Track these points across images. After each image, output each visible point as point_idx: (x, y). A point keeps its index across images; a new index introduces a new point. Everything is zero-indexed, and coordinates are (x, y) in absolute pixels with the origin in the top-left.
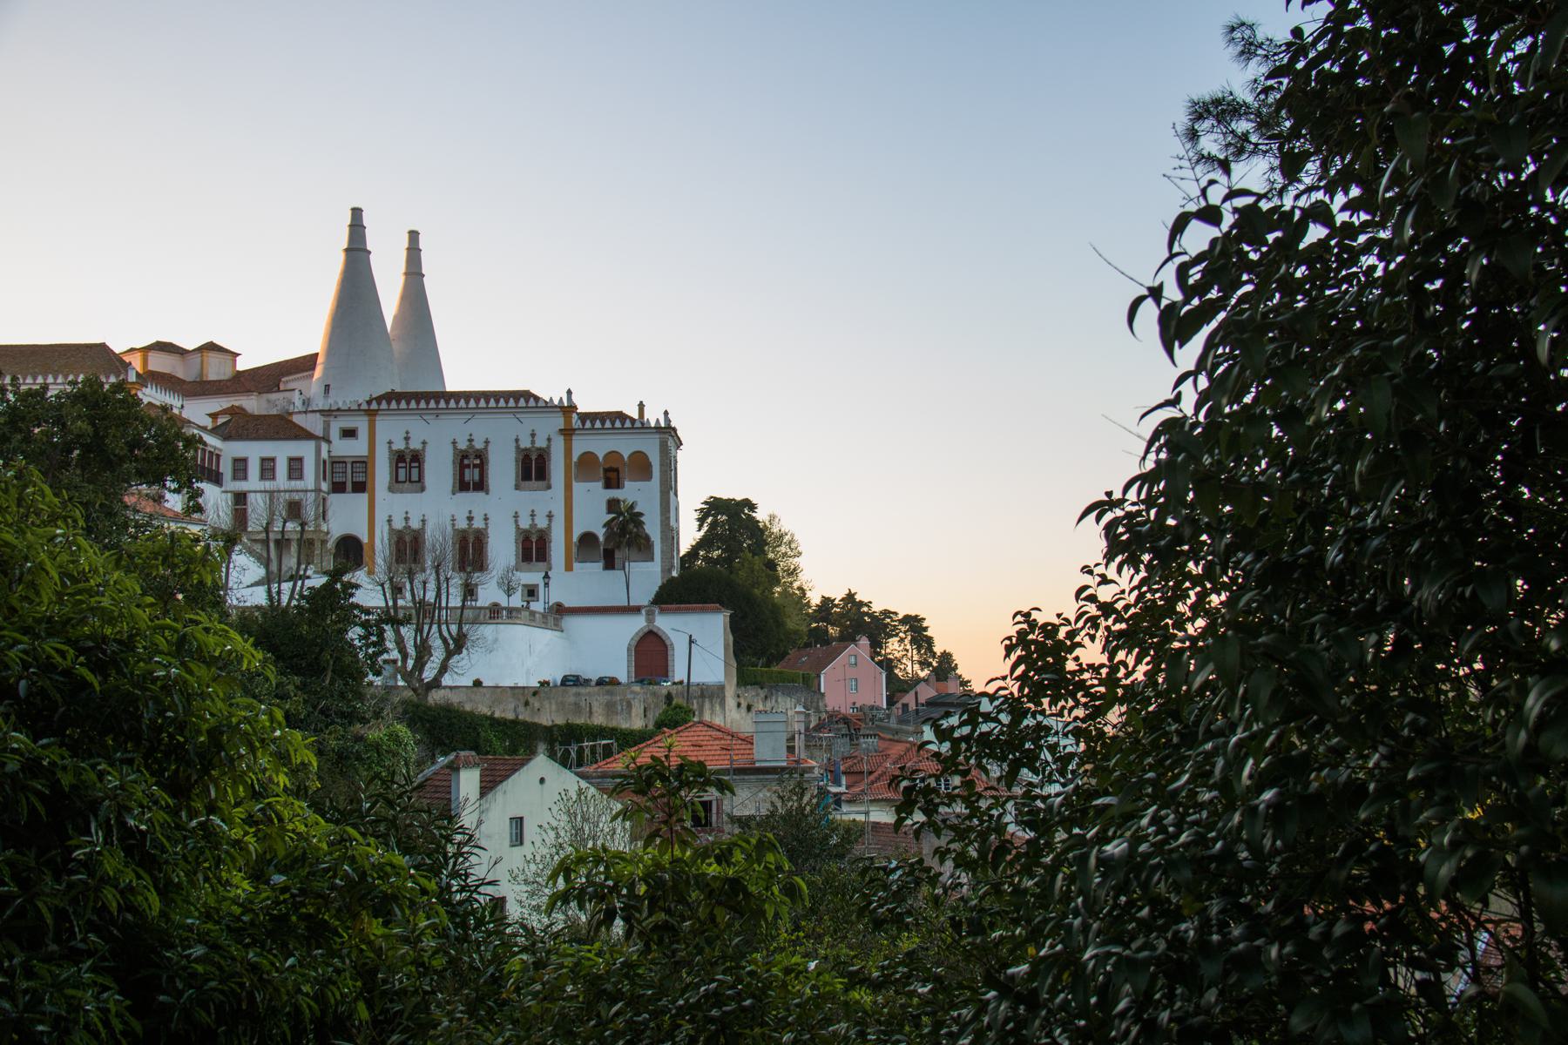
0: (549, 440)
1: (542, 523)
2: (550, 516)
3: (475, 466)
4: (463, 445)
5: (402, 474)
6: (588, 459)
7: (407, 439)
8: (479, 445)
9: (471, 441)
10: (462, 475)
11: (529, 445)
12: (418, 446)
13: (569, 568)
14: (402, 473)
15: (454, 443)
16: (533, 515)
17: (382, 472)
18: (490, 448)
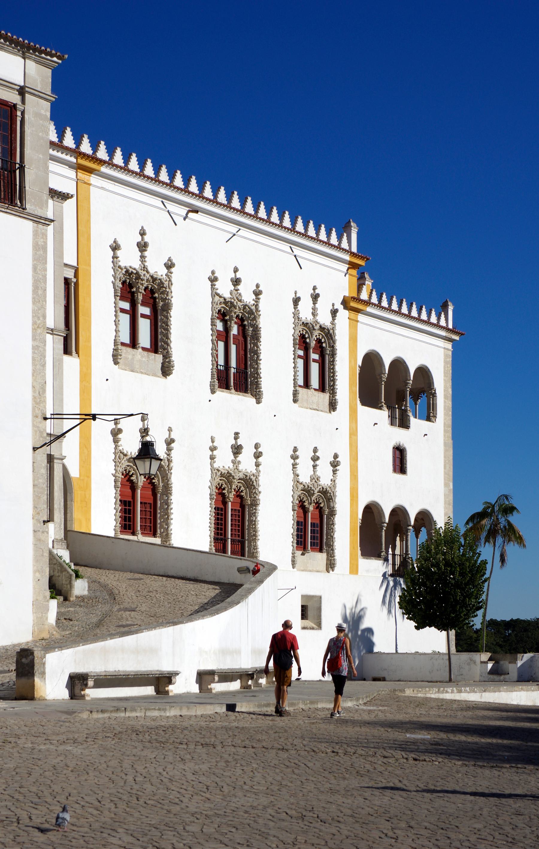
0: (334, 313)
6: (372, 360)
7: (143, 247)
9: (236, 282)
15: (213, 280)
18: (261, 307)
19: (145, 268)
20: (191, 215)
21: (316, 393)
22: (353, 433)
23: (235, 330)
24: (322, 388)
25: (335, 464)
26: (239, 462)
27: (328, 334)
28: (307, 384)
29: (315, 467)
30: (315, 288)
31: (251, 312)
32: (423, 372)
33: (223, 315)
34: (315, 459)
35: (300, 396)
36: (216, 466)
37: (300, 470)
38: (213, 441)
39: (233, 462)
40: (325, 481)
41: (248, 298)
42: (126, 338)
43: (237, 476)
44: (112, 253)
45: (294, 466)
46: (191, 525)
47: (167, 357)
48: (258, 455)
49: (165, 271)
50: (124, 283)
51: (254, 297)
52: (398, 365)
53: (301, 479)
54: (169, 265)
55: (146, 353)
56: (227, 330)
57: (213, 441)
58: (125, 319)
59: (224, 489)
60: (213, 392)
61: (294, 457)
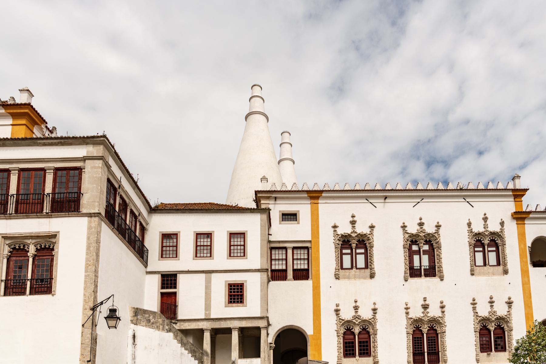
1: (501, 310)
2: (510, 303)
3: (425, 252)
4: (413, 229)
5: (347, 260)
7: (353, 223)
8: (430, 229)
9: (421, 224)
10: (411, 261)
11: (481, 230)
12: (366, 231)
14: (347, 260)
15: (404, 227)
16: (491, 302)
17: (327, 255)
18: (441, 231)
19: (354, 232)
20: (387, 200)
21: (491, 268)
26: (428, 313)
28: (485, 265)
29: (492, 306)
30: (485, 214)
31: (433, 236)
35: (475, 272)
36: (410, 316)
37: (478, 310)
38: (407, 305)
39: (423, 313)
43: (426, 319)
44: (333, 230)
45: (474, 309)
48: (442, 307)
49: (370, 230)
50: (344, 241)
51: (436, 229)
53: (480, 314)
55: (358, 270)
57: (407, 305)
59: (421, 327)
60: (406, 280)
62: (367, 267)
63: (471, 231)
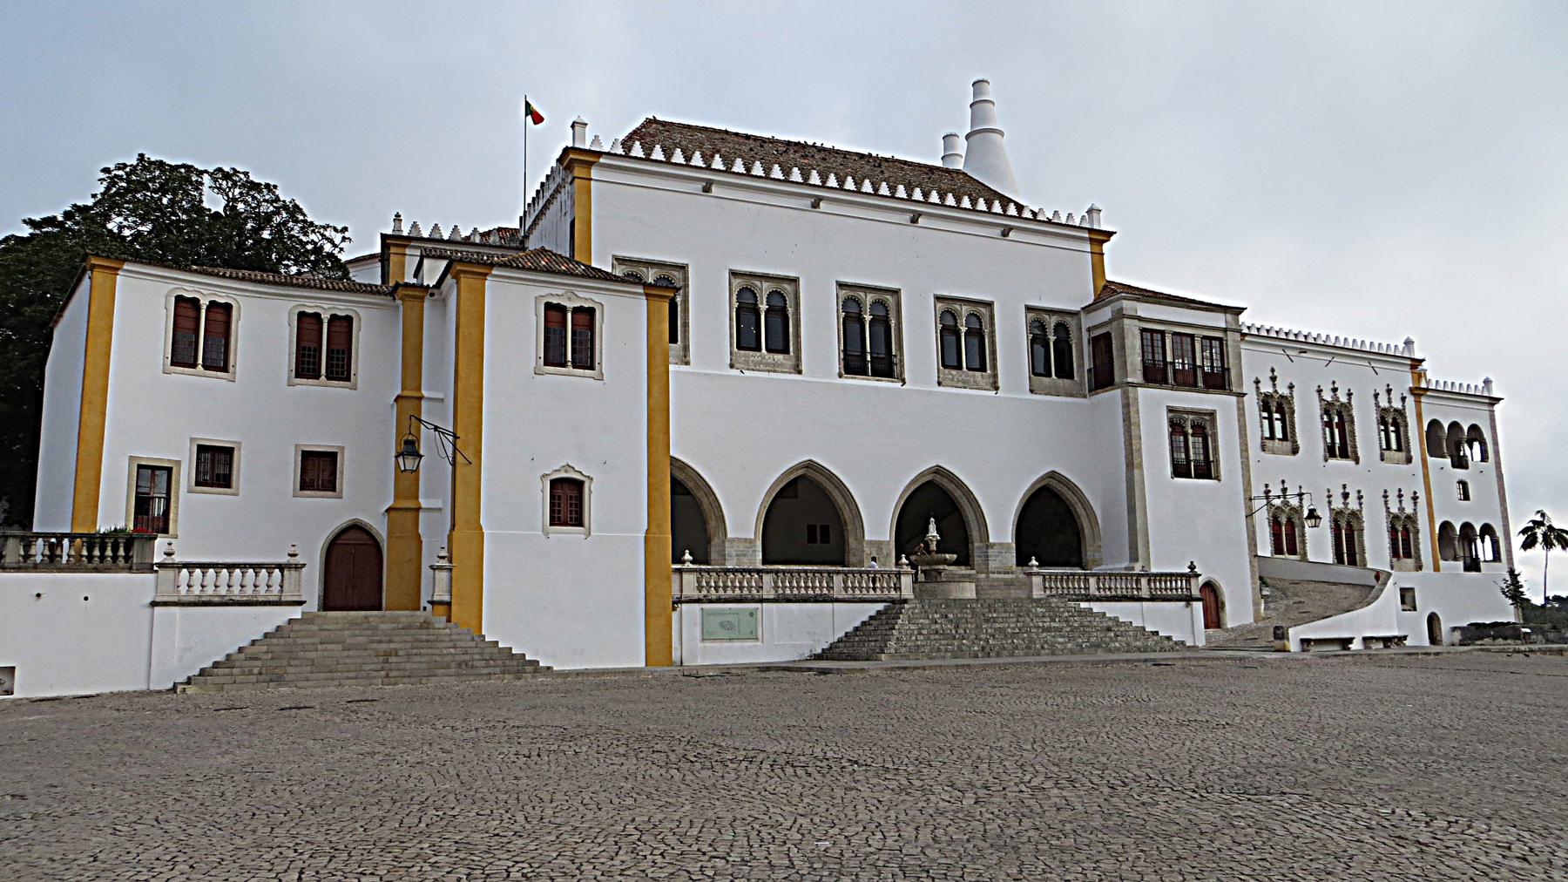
0: (1403, 399)
7: (1273, 379)
9: (1335, 390)
12: (1286, 392)
13: (1437, 569)
15: (1320, 391)
22: (1426, 476)
23: (1336, 420)
24: (1399, 449)
25: (1415, 498)
27: (1401, 413)
32: (1474, 428)
33: (1327, 412)
34: (1400, 496)
40: (1409, 510)
41: (1344, 399)
42: (1267, 434)
46: (1319, 543)
47: (1295, 442)
48: (1360, 498)
52: (1455, 426)
54: (1291, 387)
56: (1331, 420)
58: (1266, 422)
61: (1385, 497)
62: (1285, 438)
63: (1377, 405)
